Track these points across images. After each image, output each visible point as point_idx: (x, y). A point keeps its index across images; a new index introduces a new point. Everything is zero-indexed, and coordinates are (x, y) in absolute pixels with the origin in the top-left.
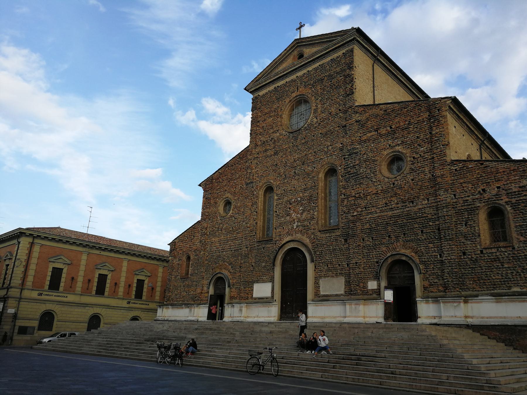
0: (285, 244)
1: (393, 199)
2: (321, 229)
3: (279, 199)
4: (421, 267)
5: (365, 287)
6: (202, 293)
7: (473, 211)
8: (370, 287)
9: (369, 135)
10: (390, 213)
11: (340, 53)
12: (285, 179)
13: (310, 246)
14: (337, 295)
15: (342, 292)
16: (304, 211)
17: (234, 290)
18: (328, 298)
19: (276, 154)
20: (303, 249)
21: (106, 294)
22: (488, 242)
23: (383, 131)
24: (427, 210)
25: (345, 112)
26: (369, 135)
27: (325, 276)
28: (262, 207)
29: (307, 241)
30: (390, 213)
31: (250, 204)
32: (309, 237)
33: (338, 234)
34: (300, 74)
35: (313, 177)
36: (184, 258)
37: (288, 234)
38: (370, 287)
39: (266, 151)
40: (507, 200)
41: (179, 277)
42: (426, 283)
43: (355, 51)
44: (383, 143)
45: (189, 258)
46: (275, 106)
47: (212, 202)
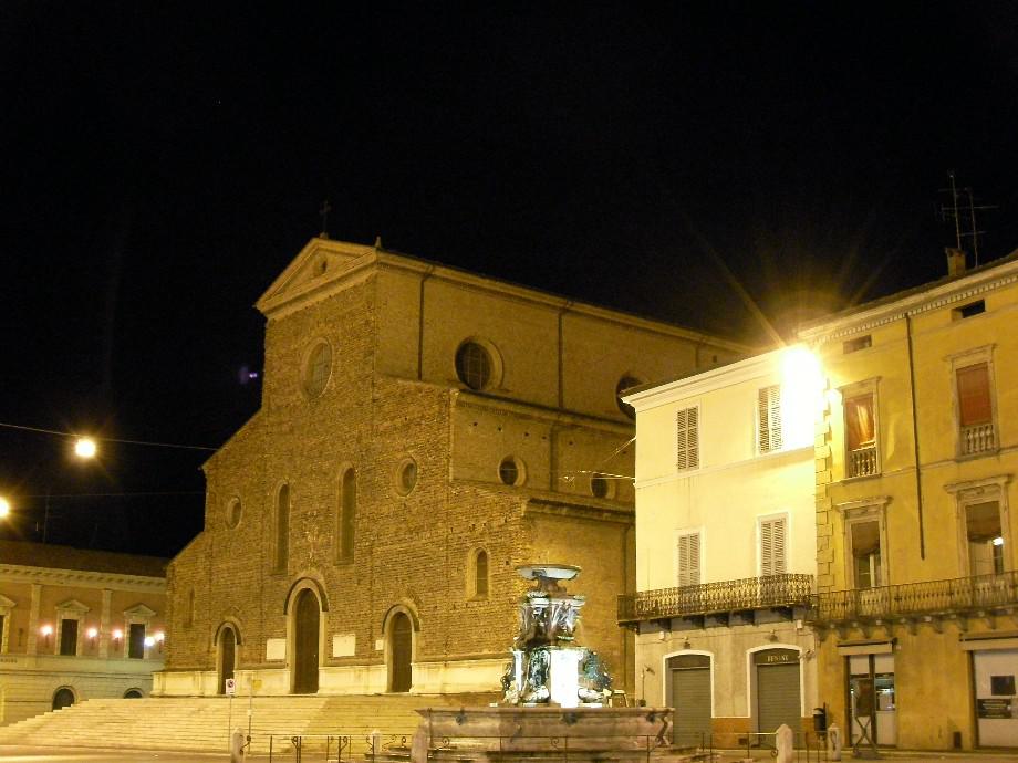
0: (300, 580)
1: (403, 526)
2: (337, 562)
3: (294, 509)
4: (421, 622)
5: (373, 647)
6: (208, 652)
7: (463, 552)
8: (377, 648)
9: (386, 424)
10: (398, 547)
11: (363, 277)
12: (301, 476)
13: (325, 588)
14: (348, 657)
15: (353, 654)
16: (320, 531)
17: (245, 648)
18: (342, 661)
19: (292, 431)
20: (316, 591)
21: (79, 652)
22: (474, 593)
23: (398, 422)
24: (430, 547)
25: (364, 381)
26: (386, 424)
27: (339, 631)
28: (277, 519)
29: (321, 580)
30: (398, 547)
31: (261, 512)
32: (323, 573)
33: (351, 571)
34: (321, 297)
35: (331, 480)
36: (186, 594)
37: (304, 567)
38: (377, 648)
39: (281, 423)
40: (489, 541)
41: (181, 625)
42: (423, 643)
43: (380, 280)
44: (400, 441)
45: (192, 594)
46: (292, 347)
47: (218, 500)
